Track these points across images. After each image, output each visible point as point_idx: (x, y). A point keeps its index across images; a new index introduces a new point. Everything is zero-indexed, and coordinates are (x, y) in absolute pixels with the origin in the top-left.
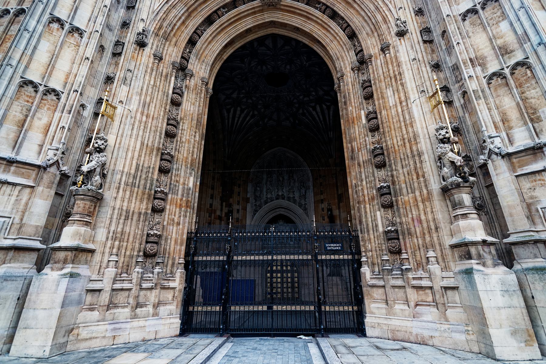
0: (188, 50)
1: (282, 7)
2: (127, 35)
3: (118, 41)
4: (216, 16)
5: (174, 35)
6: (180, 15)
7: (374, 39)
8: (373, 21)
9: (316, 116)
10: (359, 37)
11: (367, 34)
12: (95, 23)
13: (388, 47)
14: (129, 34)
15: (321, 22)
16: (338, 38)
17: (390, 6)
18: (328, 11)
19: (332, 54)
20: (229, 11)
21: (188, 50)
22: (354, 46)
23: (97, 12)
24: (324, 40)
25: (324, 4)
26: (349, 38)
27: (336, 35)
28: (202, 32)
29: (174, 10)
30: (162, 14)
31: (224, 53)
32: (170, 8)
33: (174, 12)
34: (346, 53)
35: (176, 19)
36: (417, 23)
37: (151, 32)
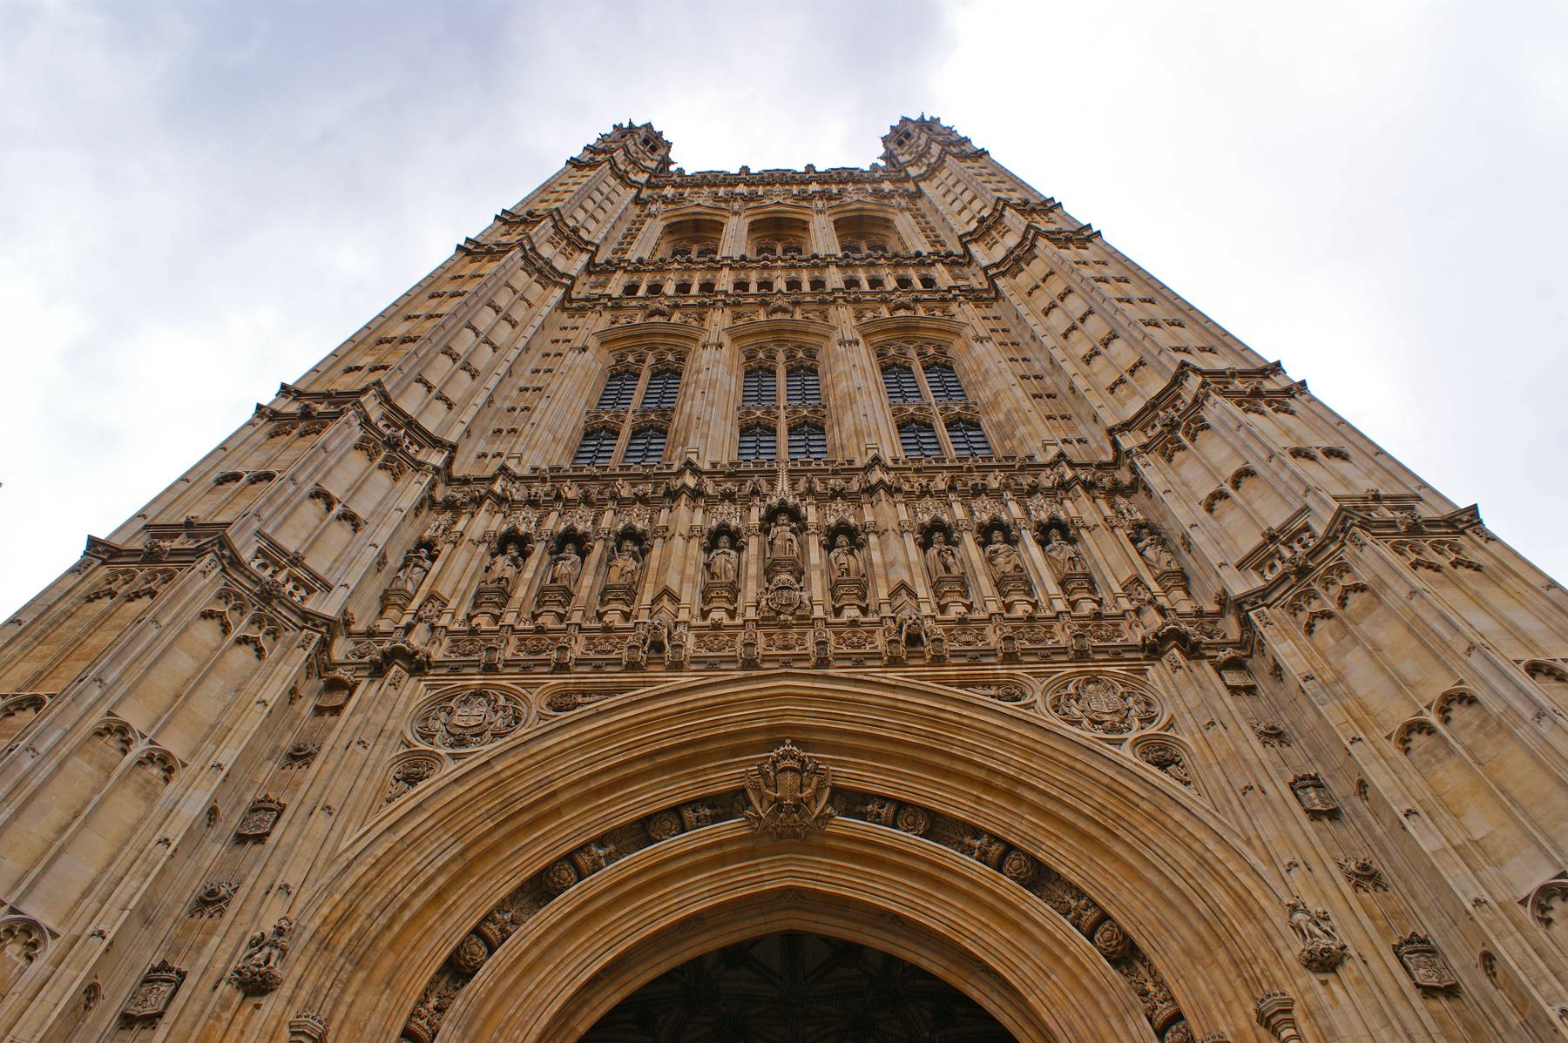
0: (433, 1002)
2: (204, 943)
3: (164, 966)
4: (567, 873)
5: (391, 946)
6: (431, 871)
7: (1217, 974)
8: (1201, 906)
10: (1158, 962)
11: (1188, 952)
12: (103, 903)
14: (215, 941)
15: (989, 899)
16: (1068, 961)
17: (1253, 859)
18: (1013, 862)
19: (1052, 1024)
20: (620, 853)
21: (433, 1002)
22: (1144, 994)
23: (127, 863)
24: (1013, 968)
25: (996, 838)
26: (1115, 963)
27: (1058, 952)
28: (502, 930)
29: (414, 854)
30: (363, 869)
31: (580, 1007)
32: (399, 848)
33: (415, 859)
34: (1114, 1022)
35: (413, 887)
36: (1372, 917)
37: (307, 935)
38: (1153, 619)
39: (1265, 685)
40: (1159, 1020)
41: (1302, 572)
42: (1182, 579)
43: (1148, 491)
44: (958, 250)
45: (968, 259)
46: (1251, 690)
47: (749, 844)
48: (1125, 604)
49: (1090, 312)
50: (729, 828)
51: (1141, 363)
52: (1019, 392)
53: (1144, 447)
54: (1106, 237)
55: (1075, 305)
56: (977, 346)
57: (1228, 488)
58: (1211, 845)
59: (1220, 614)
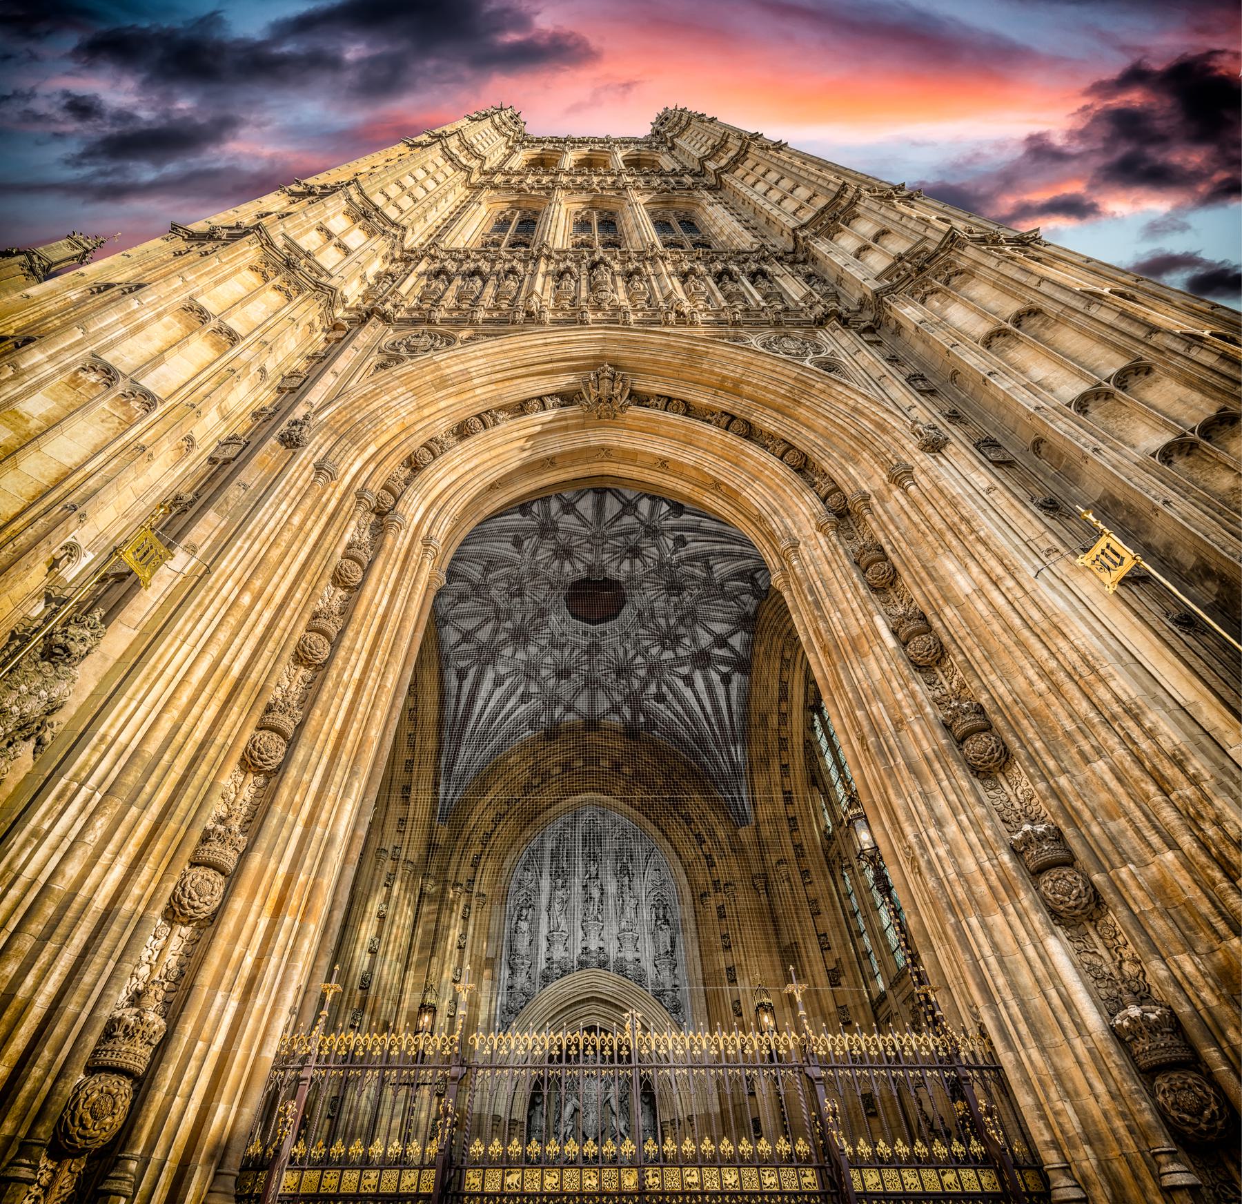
1: (629, 421)
9: (693, 701)
13: (909, 472)
38: (819, 309)
39: (887, 342)
40: (823, 493)
41: (921, 270)
42: (836, 297)
43: (815, 260)
44: (698, 169)
45: (703, 172)
46: (879, 343)
47: (581, 421)
48: (802, 304)
49: (782, 178)
50: (571, 410)
51: (815, 195)
52: (736, 224)
53: (815, 234)
54: (790, 145)
55: (773, 176)
56: (710, 209)
57: (870, 242)
58: (860, 400)
59: (860, 311)
